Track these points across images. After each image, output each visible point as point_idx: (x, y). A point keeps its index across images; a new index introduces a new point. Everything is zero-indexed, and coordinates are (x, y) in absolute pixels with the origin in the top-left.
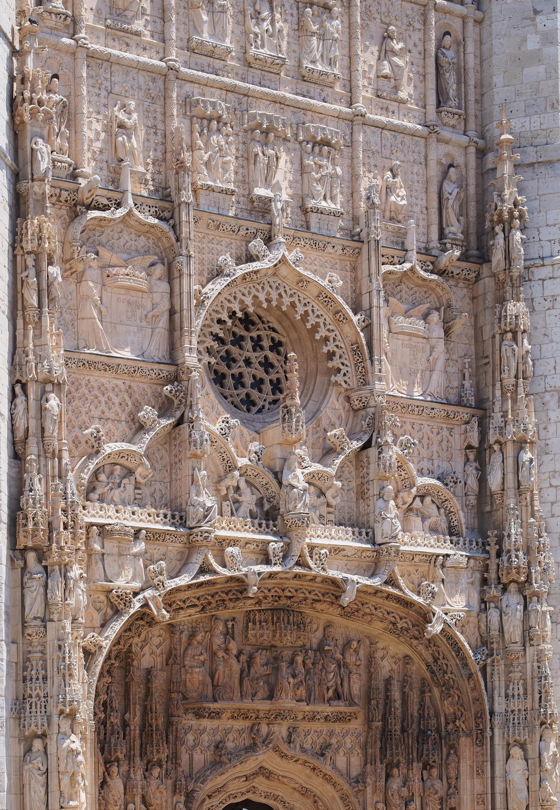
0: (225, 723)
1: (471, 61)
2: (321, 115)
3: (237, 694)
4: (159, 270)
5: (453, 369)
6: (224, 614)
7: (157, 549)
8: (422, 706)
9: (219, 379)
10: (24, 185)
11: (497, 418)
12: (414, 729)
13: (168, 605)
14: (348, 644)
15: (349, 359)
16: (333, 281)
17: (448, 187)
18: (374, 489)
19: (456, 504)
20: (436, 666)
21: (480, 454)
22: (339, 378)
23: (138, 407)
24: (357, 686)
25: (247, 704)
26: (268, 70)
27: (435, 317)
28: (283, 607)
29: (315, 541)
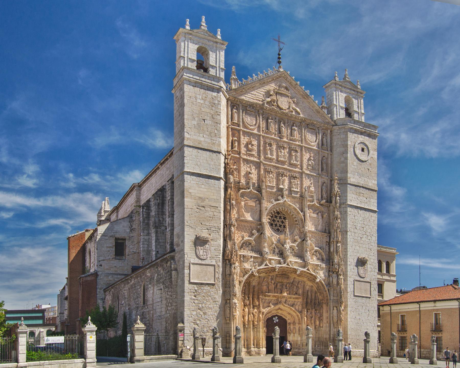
3: (274, 292)
4: (257, 202)
5: (324, 225)
9: (271, 225)
10: (227, 185)
16: (297, 206)
22: (298, 226)
23: (252, 230)
27: (320, 214)
29: (291, 260)
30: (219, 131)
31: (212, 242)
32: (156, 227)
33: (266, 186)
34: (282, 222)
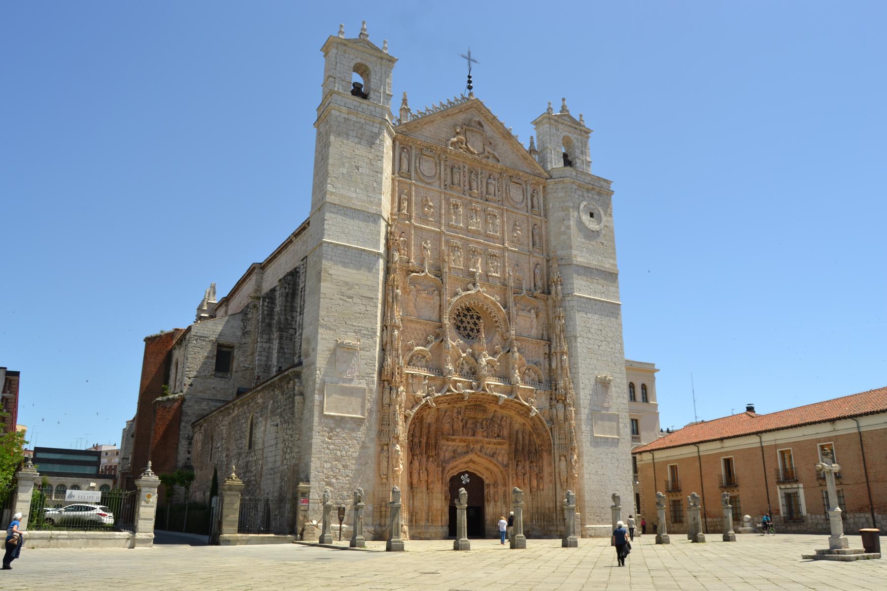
0: (457, 443)
1: (544, 233)
2: (494, 247)
5: (540, 328)
6: (457, 406)
7: (432, 383)
8: (530, 441)
10: (389, 265)
11: (554, 345)
12: (527, 449)
13: (436, 402)
14: (502, 418)
15: (502, 323)
16: (496, 298)
17: (537, 271)
18: (511, 367)
19: (541, 372)
20: (534, 427)
21: (549, 356)
23: (428, 335)
24: (505, 432)
25: (465, 437)
26: (476, 233)
27: (533, 311)
28: (478, 404)
30: (380, 183)
31: (362, 352)
32: (280, 330)
33: (450, 268)
34: (475, 324)
